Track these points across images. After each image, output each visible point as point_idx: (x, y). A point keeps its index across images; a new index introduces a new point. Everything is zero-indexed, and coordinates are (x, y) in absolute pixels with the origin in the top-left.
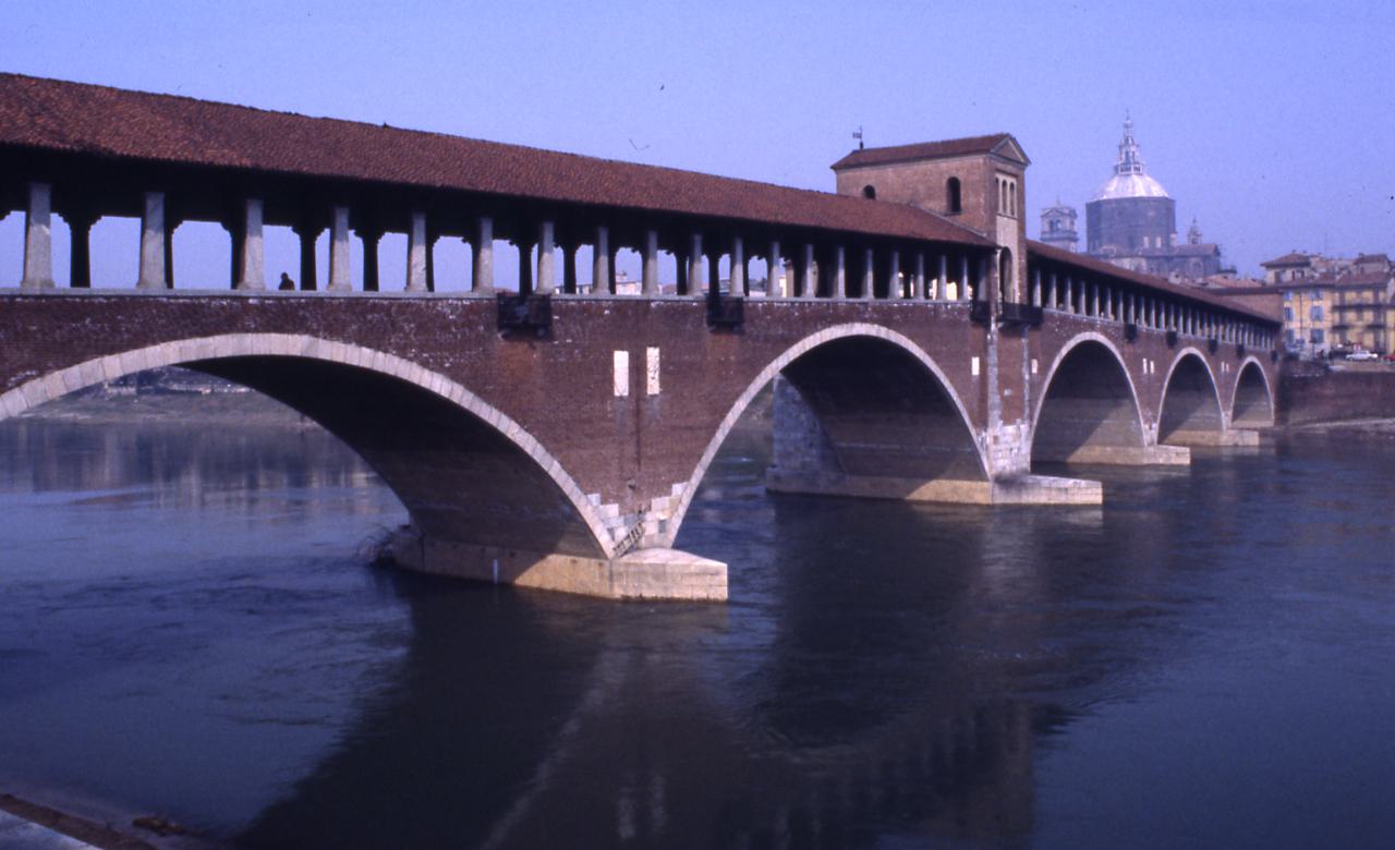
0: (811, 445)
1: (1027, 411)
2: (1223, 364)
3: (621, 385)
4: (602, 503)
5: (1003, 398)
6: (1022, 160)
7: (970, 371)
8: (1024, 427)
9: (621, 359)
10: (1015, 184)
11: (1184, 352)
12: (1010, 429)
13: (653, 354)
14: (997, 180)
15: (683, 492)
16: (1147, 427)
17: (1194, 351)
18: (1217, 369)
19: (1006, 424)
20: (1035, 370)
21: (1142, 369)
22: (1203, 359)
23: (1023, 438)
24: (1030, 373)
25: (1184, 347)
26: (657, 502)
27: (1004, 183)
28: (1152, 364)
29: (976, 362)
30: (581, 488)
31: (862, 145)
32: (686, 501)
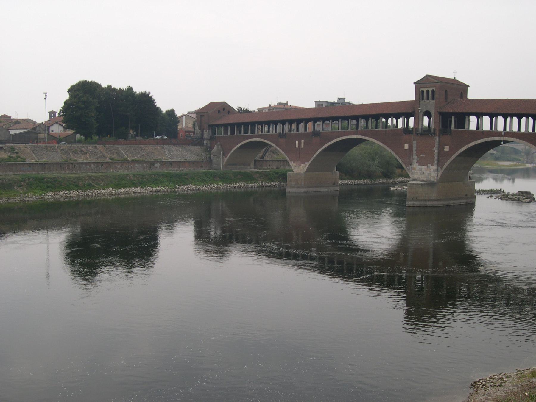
1: (436, 162)
3: (297, 146)
5: (419, 156)
6: (437, 81)
8: (435, 167)
9: (297, 142)
10: (434, 89)
12: (424, 167)
13: (303, 141)
14: (423, 91)
15: (308, 164)
19: (419, 165)
23: (432, 170)
26: (302, 165)
27: (428, 91)
30: (290, 160)
31: (455, 77)
32: (308, 166)
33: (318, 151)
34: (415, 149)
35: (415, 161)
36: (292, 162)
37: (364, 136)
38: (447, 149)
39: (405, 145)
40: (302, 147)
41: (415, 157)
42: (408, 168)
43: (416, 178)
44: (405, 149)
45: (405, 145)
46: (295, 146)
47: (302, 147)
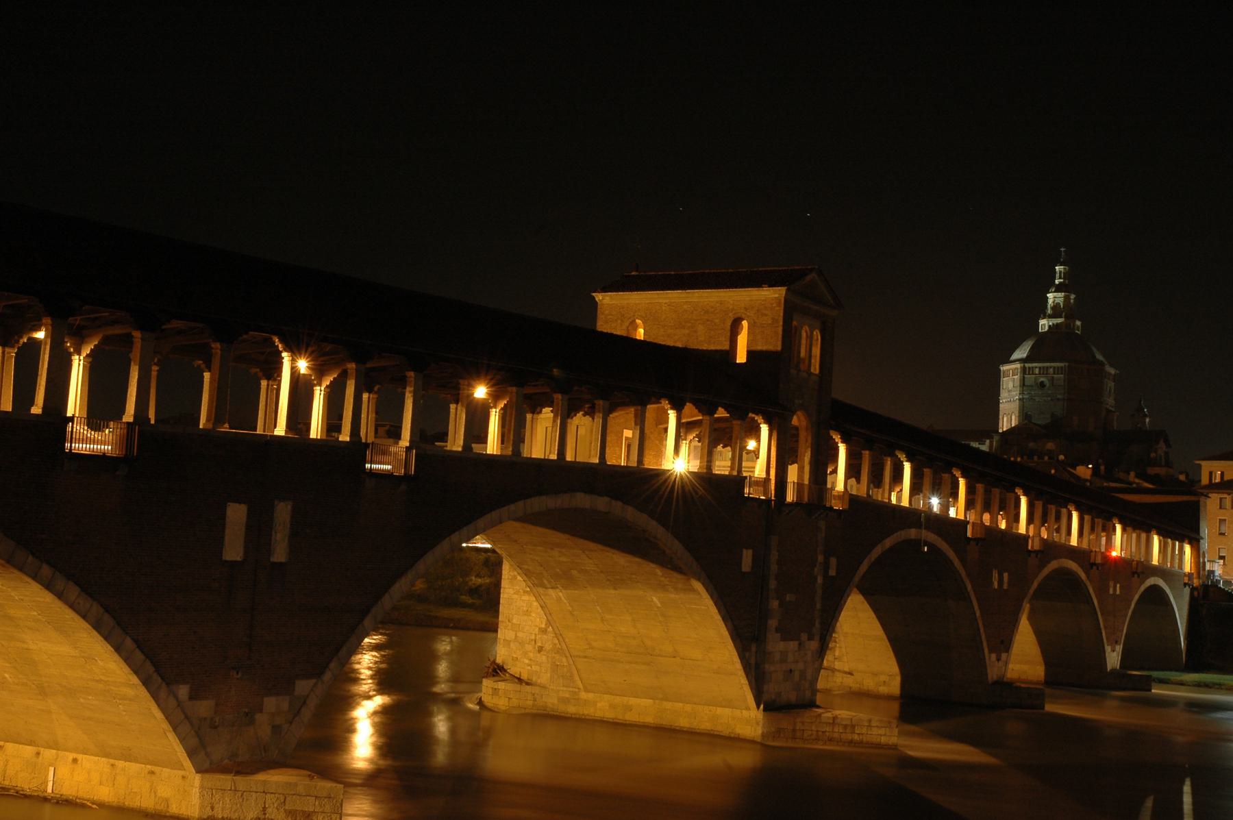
0: (540, 649)
2: (1111, 584)
3: (233, 551)
4: (191, 698)
7: (739, 564)
9: (236, 514)
11: (1054, 565)
12: (793, 645)
13: (283, 512)
16: (994, 656)
17: (1072, 565)
18: (1102, 591)
19: (781, 641)
20: (832, 573)
21: (992, 583)
22: (1083, 576)
24: (826, 576)
25: (1055, 558)
26: (270, 703)
28: (1006, 575)
29: (747, 556)
33: (397, 586)
34: (774, 568)
35: (773, 623)
36: (183, 691)
37: (619, 504)
38: (832, 573)
39: (745, 551)
40: (280, 554)
41: (774, 604)
42: (747, 654)
43: (773, 697)
44: (743, 570)
45: (745, 551)
46: (219, 542)
47: (280, 554)
